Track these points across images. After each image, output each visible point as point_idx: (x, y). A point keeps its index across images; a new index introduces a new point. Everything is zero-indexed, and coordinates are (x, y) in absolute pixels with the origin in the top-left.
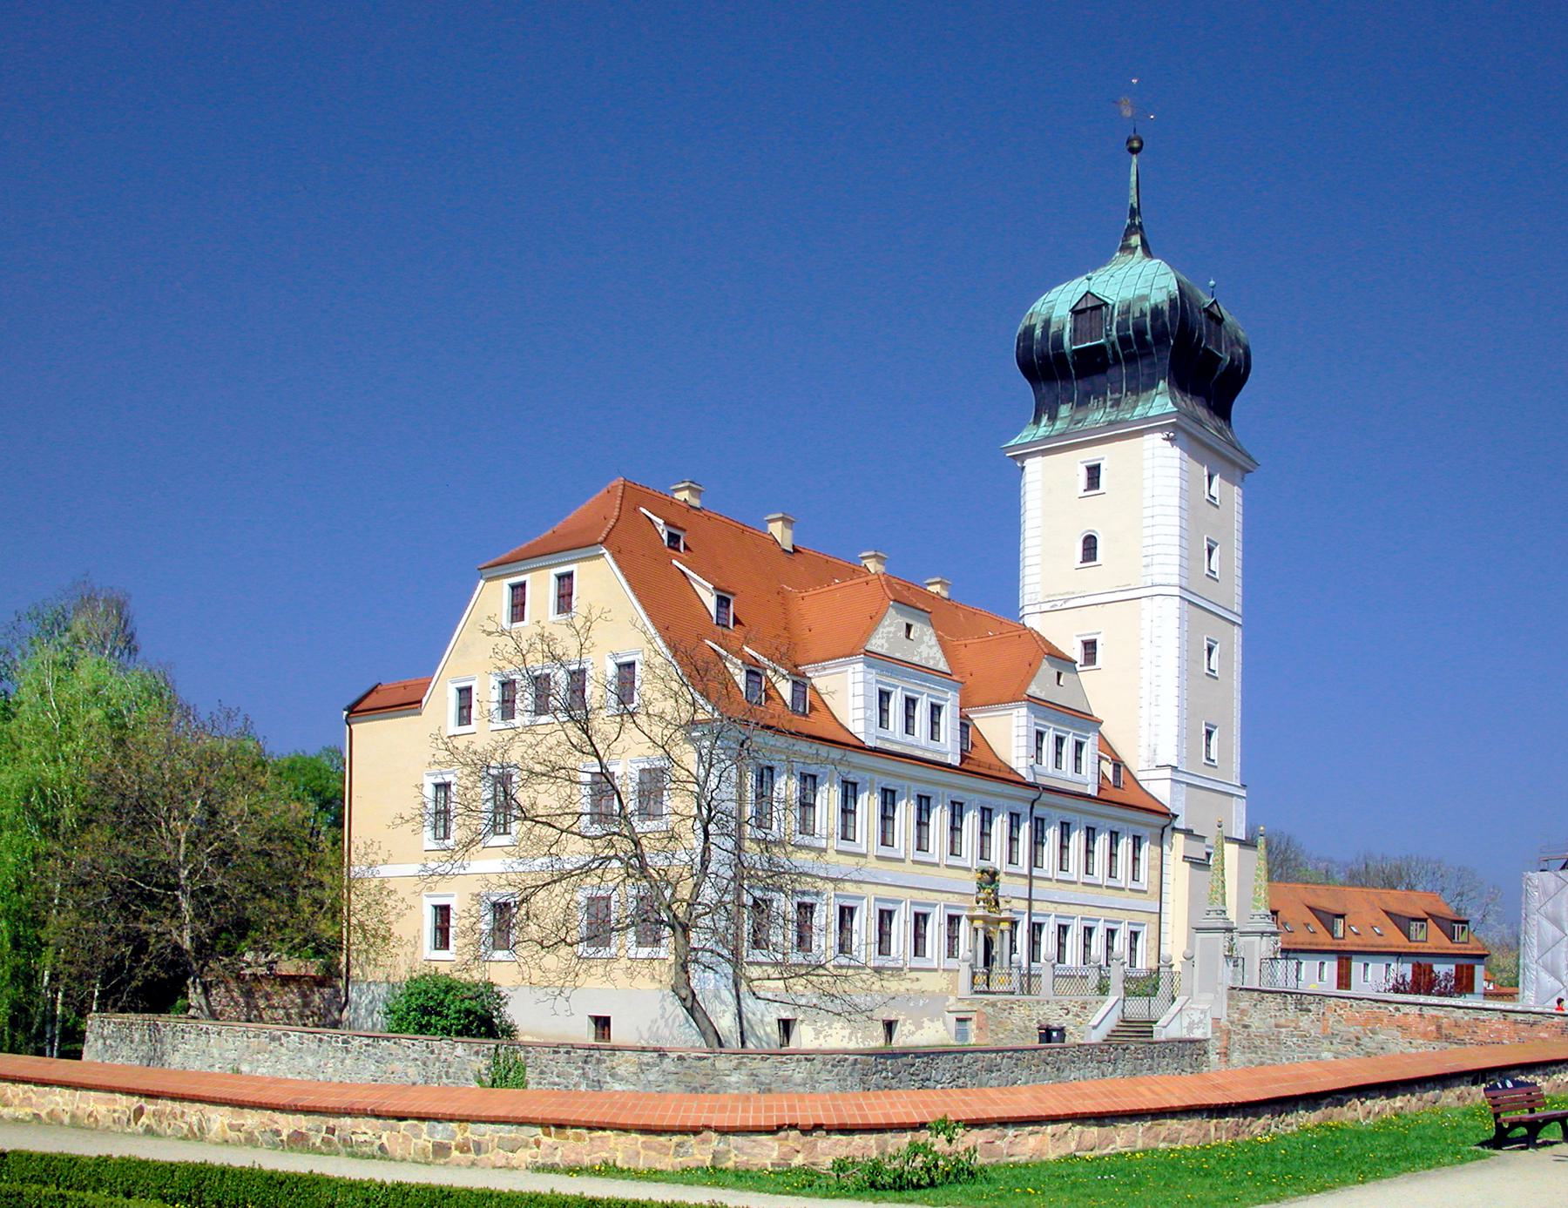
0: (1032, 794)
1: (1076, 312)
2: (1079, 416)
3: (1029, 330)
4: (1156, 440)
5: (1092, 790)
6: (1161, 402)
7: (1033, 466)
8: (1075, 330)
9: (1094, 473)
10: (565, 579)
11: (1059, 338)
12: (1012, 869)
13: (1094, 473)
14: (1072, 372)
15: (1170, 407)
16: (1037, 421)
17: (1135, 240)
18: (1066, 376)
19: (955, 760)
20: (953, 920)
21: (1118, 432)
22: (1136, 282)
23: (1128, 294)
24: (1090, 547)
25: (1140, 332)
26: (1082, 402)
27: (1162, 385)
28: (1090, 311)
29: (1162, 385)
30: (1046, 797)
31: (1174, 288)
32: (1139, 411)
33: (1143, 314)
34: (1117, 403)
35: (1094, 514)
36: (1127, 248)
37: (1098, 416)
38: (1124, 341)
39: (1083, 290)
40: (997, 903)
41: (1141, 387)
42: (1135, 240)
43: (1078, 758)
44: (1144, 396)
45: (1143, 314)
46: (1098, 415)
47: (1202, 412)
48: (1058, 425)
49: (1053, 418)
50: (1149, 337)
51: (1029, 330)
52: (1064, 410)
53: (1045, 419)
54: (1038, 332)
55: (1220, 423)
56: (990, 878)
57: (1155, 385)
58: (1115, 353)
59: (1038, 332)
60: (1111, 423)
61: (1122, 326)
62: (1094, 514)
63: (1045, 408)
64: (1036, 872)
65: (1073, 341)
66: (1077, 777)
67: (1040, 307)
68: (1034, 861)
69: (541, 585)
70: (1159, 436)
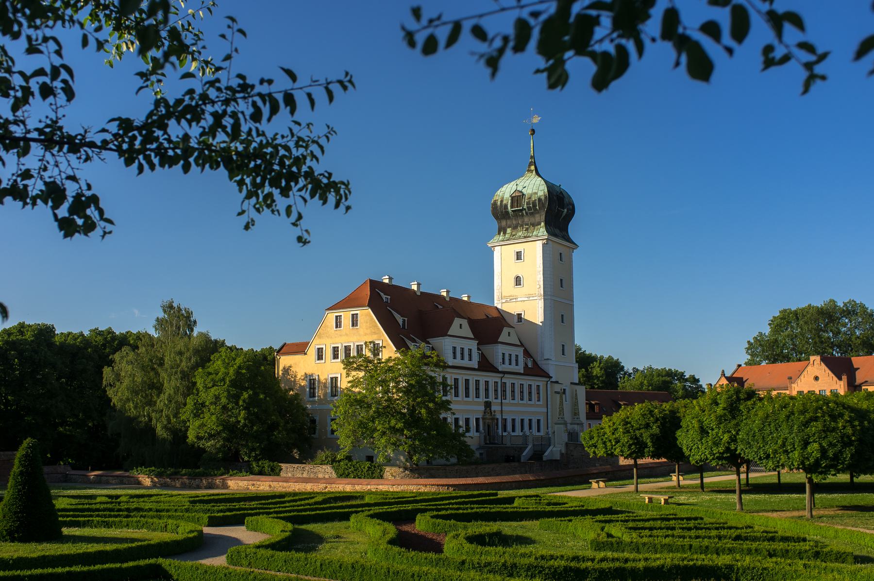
0: (501, 375)
1: (512, 198)
3: (495, 203)
7: (497, 251)
9: (519, 256)
10: (354, 318)
11: (506, 206)
12: (495, 401)
14: (510, 218)
16: (499, 234)
18: (509, 218)
19: (477, 367)
20: (477, 420)
22: (533, 186)
26: (515, 228)
28: (517, 198)
31: (546, 190)
32: (535, 233)
34: (527, 229)
35: (518, 269)
36: (530, 171)
38: (529, 208)
39: (514, 188)
42: (533, 168)
46: (520, 234)
47: (557, 231)
49: (505, 233)
51: (495, 203)
52: (509, 230)
54: (499, 203)
56: (488, 405)
61: (528, 203)
62: (518, 269)
63: (502, 230)
67: (500, 193)
68: (504, 396)
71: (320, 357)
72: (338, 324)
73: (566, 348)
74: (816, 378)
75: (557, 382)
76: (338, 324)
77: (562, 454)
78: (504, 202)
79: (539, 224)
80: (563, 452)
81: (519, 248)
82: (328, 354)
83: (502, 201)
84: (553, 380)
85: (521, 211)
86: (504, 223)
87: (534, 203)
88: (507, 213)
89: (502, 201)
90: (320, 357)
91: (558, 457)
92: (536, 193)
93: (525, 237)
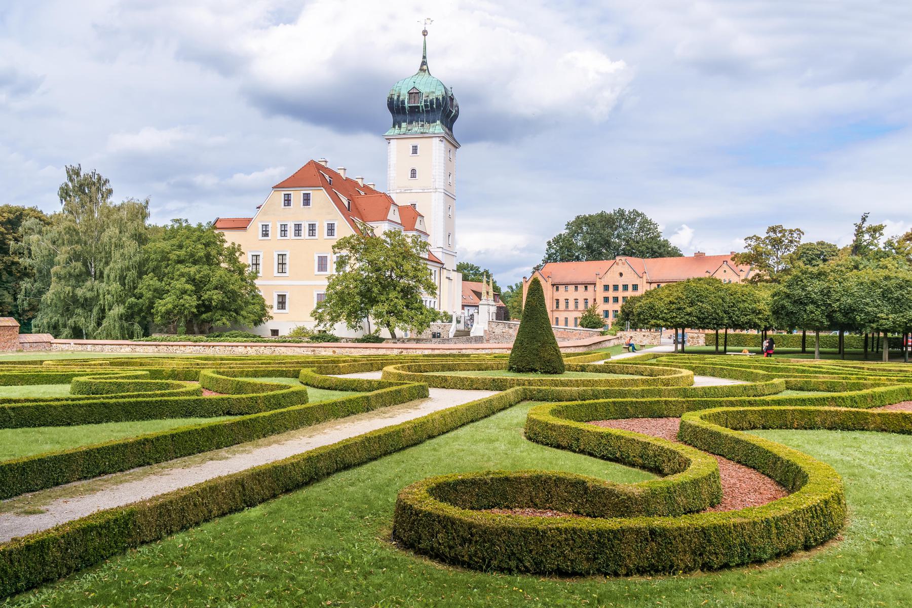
1: (410, 94)
6: (438, 128)
8: (409, 99)
9: (415, 150)
13: (415, 150)
16: (394, 126)
17: (425, 67)
21: (423, 136)
23: (428, 90)
24: (413, 173)
26: (411, 123)
27: (438, 122)
29: (438, 122)
32: (431, 130)
37: (416, 128)
38: (426, 106)
46: (416, 129)
48: (403, 130)
49: (400, 127)
52: (404, 125)
54: (396, 98)
57: (435, 122)
60: (422, 133)
61: (426, 101)
63: (397, 123)
65: (409, 103)
69: (297, 196)
70: (438, 139)
71: (265, 234)
72: (288, 201)
74: (621, 274)
76: (288, 201)
77: (485, 331)
78: (401, 98)
80: (486, 328)
83: (399, 96)
86: (399, 118)
87: (432, 102)
88: (404, 108)
89: (399, 96)
90: (265, 234)
92: (433, 92)
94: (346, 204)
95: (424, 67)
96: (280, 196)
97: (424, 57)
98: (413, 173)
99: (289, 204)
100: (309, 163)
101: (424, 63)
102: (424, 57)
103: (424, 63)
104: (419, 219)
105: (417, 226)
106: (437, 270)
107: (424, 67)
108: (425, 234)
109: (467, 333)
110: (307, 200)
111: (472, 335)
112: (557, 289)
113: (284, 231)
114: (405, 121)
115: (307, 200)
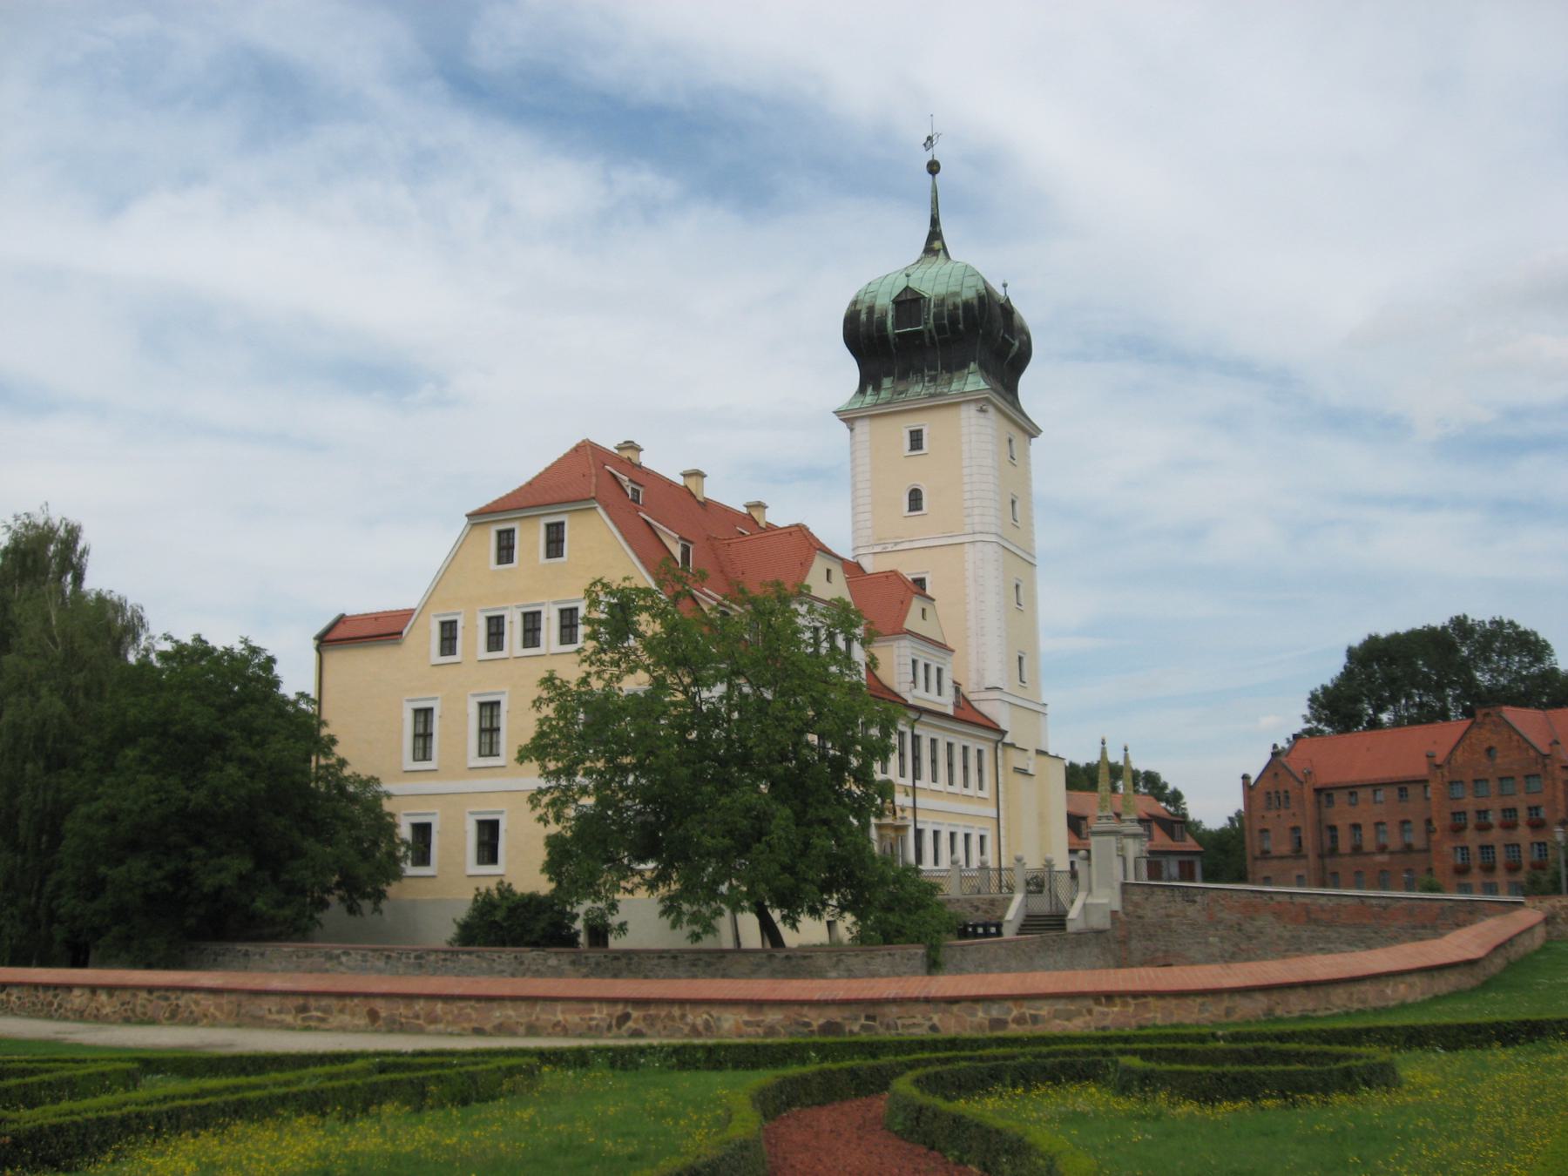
2: (900, 388)
4: (968, 414)
5: (950, 711)
6: (974, 382)
9: (916, 440)
11: (882, 323)
13: (916, 440)
15: (983, 385)
17: (937, 245)
24: (915, 500)
25: (953, 320)
26: (903, 376)
29: (973, 366)
30: (924, 718)
32: (955, 386)
33: (956, 307)
38: (940, 328)
40: (895, 813)
41: (955, 366)
43: (939, 683)
44: (957, 374)
45: (956, 307)
46: (918, 388)
47: (1000, 388)
48: (883, 394)
50: (961, 326)
52: (887, 383)
53: (870, 390)
54: (863, 317)
55: (1010, 397)
58: (932, 338)
59: (863, 317)
64: (918, 783)
65: (897, 325)
66: (938, 699)
68: (916, 775)
72: (505, 551)
73: (1025, 662)
75: (1012, 745)
76: (505, 551)
79: (963, 365)
80: (1117, 906)
81: (914, 422)
82: (473, 636)
83: (871, 310)
84: (1007, 739)
85: (920, 333)
89: (871, 310)
91: (1100, 921)
92: (956, 294)
93: (932, 396)
94: (677, 551)
95: (934, 244)
96: (489, 540)
97: (935, 222)
98: (915, 500)
99: (510, 559)
100: (577, 449)
101: (935, 234)
102: (935, 222)
103: (935, 234)
104: (916, 605)
105: (912, 621)
106: (988, 749)
107: (934, 244)
108: (942, 646)
109: (1057, 921)
110: (555, 545)
111: (1070, 927)
112: (1330, 802)
113: (495, 635)
114: (887, 375)
115: (555, 545)
